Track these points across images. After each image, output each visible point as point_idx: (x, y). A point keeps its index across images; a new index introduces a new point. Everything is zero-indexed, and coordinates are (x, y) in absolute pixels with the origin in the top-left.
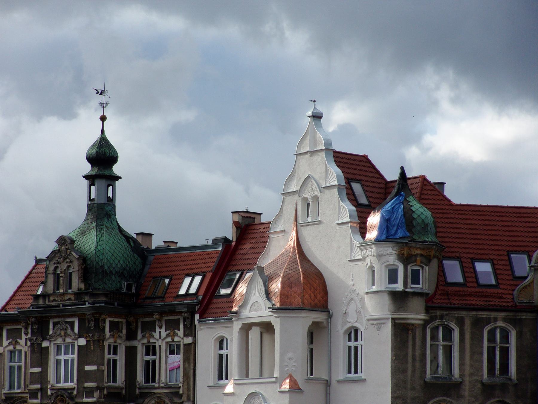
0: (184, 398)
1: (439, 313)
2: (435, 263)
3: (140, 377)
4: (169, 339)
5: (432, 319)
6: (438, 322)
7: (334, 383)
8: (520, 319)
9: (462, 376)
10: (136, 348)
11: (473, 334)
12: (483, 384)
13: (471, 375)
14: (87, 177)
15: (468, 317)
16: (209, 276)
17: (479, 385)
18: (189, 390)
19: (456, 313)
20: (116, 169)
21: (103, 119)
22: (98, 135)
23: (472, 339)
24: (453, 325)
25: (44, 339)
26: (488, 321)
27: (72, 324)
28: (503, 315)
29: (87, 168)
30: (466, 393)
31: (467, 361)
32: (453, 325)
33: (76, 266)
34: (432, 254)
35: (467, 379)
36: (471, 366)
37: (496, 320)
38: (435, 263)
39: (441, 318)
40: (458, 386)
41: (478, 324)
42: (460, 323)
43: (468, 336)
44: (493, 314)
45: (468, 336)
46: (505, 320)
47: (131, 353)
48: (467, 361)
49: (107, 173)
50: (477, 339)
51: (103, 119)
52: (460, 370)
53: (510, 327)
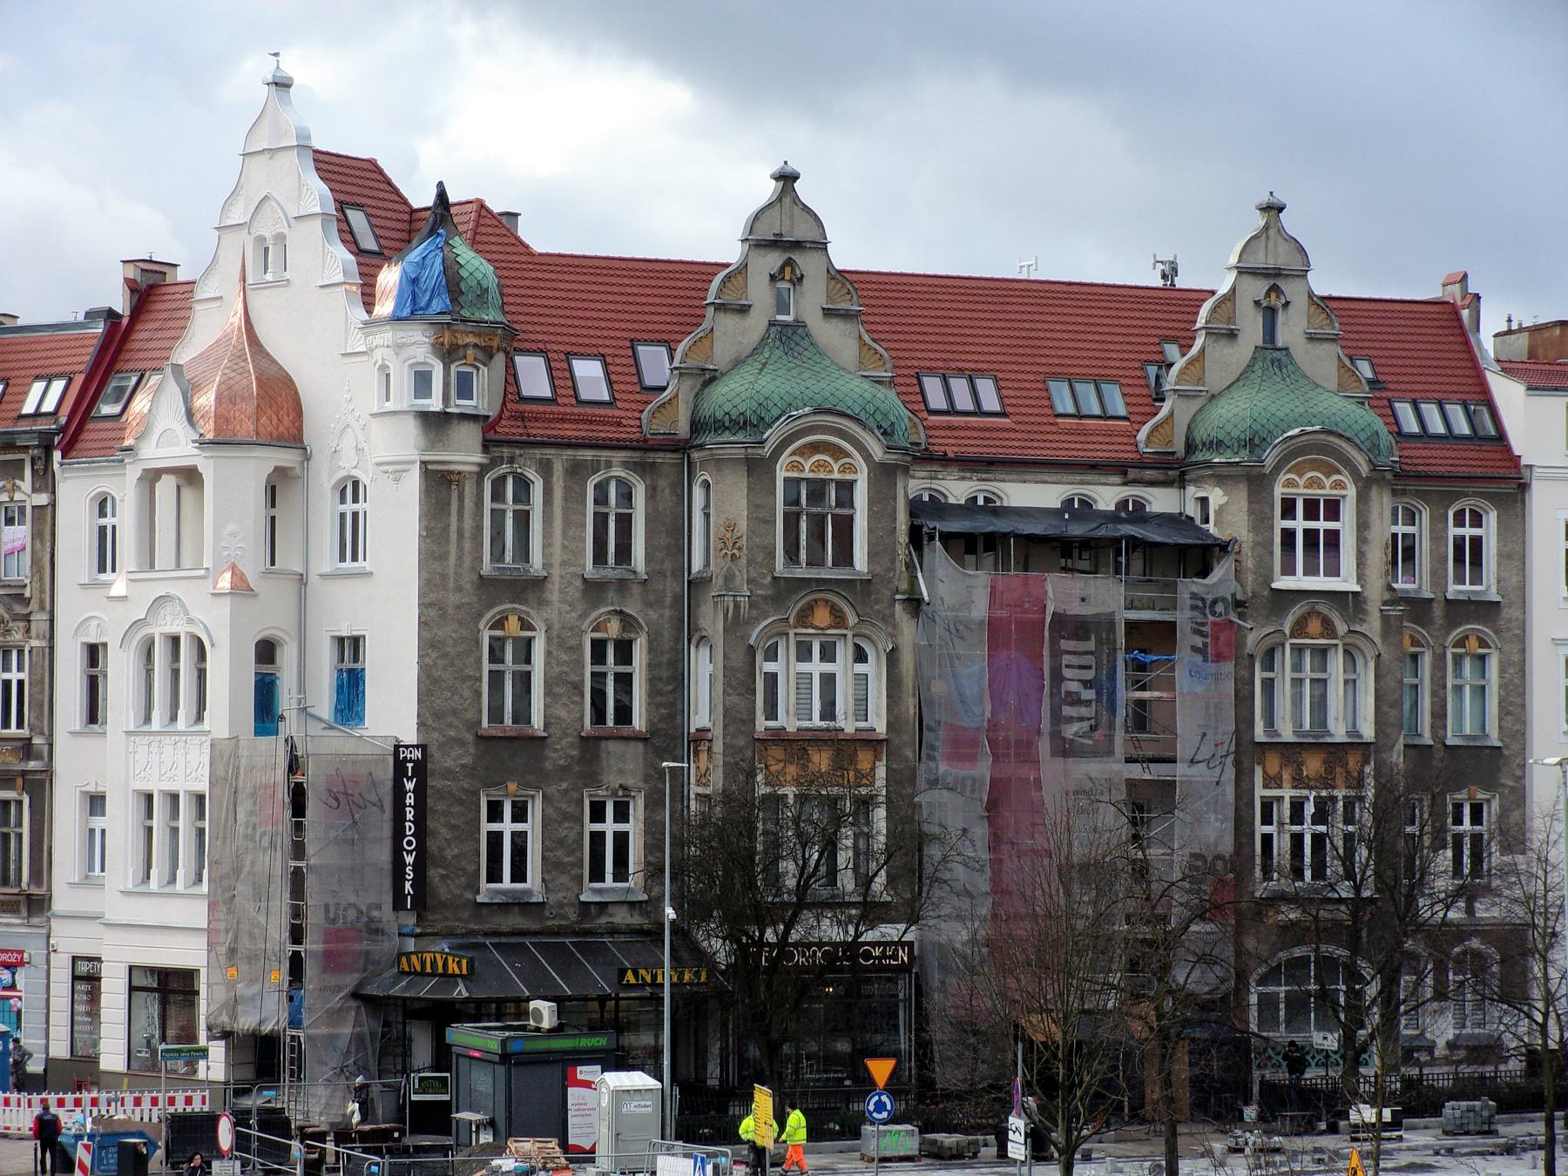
0: (34, 605)
1: (506, 452)
2: (500, 359)
5: (494, 463)
6: (504, 469)
7: (313, 578)
12: (585, 580)
13: (564, 564)
15: (560, 461)
16: (79, 380)
17: (578, 583)
18: (42, 591)
23: (566, 500)
24: (531, 474)
26: (595, 467)
28: (620, 456)
34: (495, 344)
35: (556, 572)
36: (564, 547)
37: (609, 465)
38: (500, 359)
39: (511, 460)
40: (540, 583)
41: (577, 472)
42: (545, 469)
43: (558, 494)
44: (604, 455)
45: (558, 494)
46: (626, 465)
50: (574, 498)
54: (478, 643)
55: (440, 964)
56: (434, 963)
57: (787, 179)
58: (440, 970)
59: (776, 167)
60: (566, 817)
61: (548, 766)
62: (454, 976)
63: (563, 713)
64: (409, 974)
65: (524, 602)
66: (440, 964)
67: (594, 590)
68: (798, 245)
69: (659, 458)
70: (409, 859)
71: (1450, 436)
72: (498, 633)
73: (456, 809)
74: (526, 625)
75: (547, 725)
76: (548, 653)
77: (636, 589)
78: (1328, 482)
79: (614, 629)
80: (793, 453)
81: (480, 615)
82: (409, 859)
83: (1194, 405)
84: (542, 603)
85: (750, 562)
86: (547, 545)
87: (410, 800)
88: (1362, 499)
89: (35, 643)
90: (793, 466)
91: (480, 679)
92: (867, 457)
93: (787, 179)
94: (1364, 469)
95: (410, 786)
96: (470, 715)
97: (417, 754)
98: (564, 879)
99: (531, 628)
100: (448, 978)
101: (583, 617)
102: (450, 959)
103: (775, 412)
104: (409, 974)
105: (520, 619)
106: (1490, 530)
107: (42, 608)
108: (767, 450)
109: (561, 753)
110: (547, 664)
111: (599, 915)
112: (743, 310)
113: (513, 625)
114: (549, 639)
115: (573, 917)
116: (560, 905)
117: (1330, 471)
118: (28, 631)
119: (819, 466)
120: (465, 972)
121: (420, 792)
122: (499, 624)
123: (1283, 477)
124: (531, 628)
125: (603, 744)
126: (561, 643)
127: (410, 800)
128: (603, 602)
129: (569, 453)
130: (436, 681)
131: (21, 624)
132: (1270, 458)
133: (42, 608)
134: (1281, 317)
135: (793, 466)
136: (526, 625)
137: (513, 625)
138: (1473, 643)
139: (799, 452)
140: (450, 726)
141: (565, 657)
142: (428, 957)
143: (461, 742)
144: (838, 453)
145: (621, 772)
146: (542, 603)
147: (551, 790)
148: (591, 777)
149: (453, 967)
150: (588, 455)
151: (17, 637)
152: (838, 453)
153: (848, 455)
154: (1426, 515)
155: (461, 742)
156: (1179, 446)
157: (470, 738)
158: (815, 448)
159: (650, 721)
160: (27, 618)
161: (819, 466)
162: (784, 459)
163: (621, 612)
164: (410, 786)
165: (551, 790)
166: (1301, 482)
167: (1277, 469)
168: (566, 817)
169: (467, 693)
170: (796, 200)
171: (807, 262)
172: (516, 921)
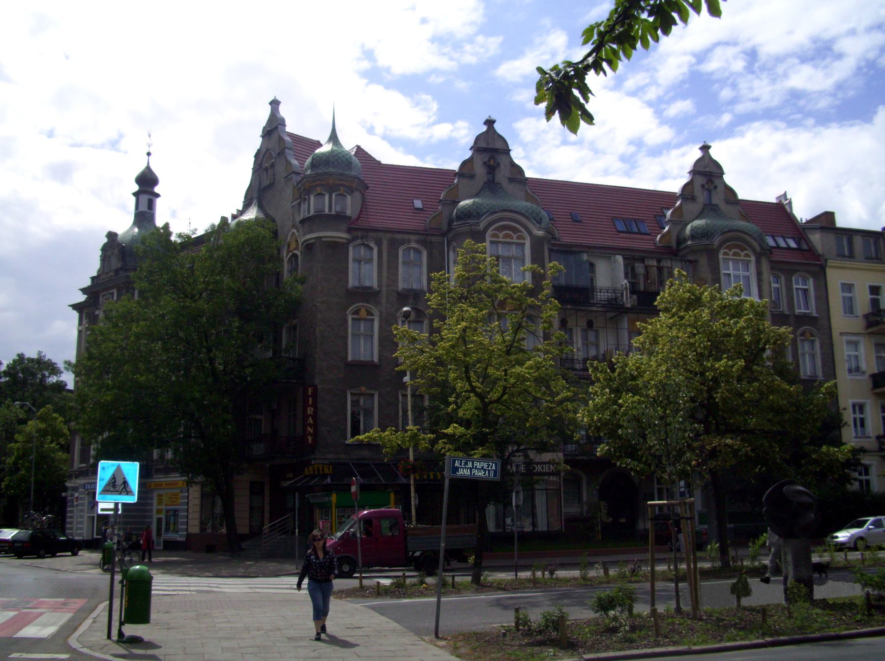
1: (360, 234)
6: (359, 241)
8: (431, 242)
9: (380, 286)
12: (398, 293)
14: (135, 194)
19: (374, 234)
20: (157, 190)
21: (149, 154)
22: (146, 165)
24: (372, 244)
25: (97, 309)
26: (403, 242)
27: (112, 294)
29: (136, 188)
30: (384, 301)
31: (385, 274)
32: (372, 244)
33: (116, 252)
34: (354, 185)
35: (384, 289)
37: (409, 241)
42: (379, 243)
43: (385, 254)
44: (406, 237)
45: (385, 254)
46: (417, 242)
48: (385, 274)
49: (148, 189)
51: (149, 154)
52: (378, 281)
54: (346, 321)
56: (318, 470)
57: (490, 123)
59: (486, 117)
65: (368, 302)
68: (496, 151)
71: (789, 248)
72: (356, 316)
75: (380, 360)
76: (381, 327)
78: (742, 254)
80: (494, 230)
81: (347, 307)
83: (679, 227)
88: (758, 262)
90: (494, 236)
91: (347, 337)
92: (530, 233)
93: (490, 123)
94: (758, 249)
99: (372, 315)
103: (484, 210)
105: (367, 310)
106: (811, 285)
108: (482, 226)
112: (472, 177)
113: (363, 313)
114: (381, 320)
117: (743, 249)
119: (506, 236)
122: (357, 312)
123: (722, 251)
124: (372, 315)
129: (389, 235)
132: (716, 241)
134: (713, 193)
135: (494, 236)
136: (369, 313)
137: (363, 313)
138: (808, 334)
139: (496, 229)
144: (515, 230)
149: (326, 470)
150: (399, 236)
152: (515, 230)
153: (520, 231)
154: (783, 279)
156: (674, 244)
162: (490, 232)
166: (731, 253)
167: (720, 246)
170: (495, 132)
171: (502, 159)
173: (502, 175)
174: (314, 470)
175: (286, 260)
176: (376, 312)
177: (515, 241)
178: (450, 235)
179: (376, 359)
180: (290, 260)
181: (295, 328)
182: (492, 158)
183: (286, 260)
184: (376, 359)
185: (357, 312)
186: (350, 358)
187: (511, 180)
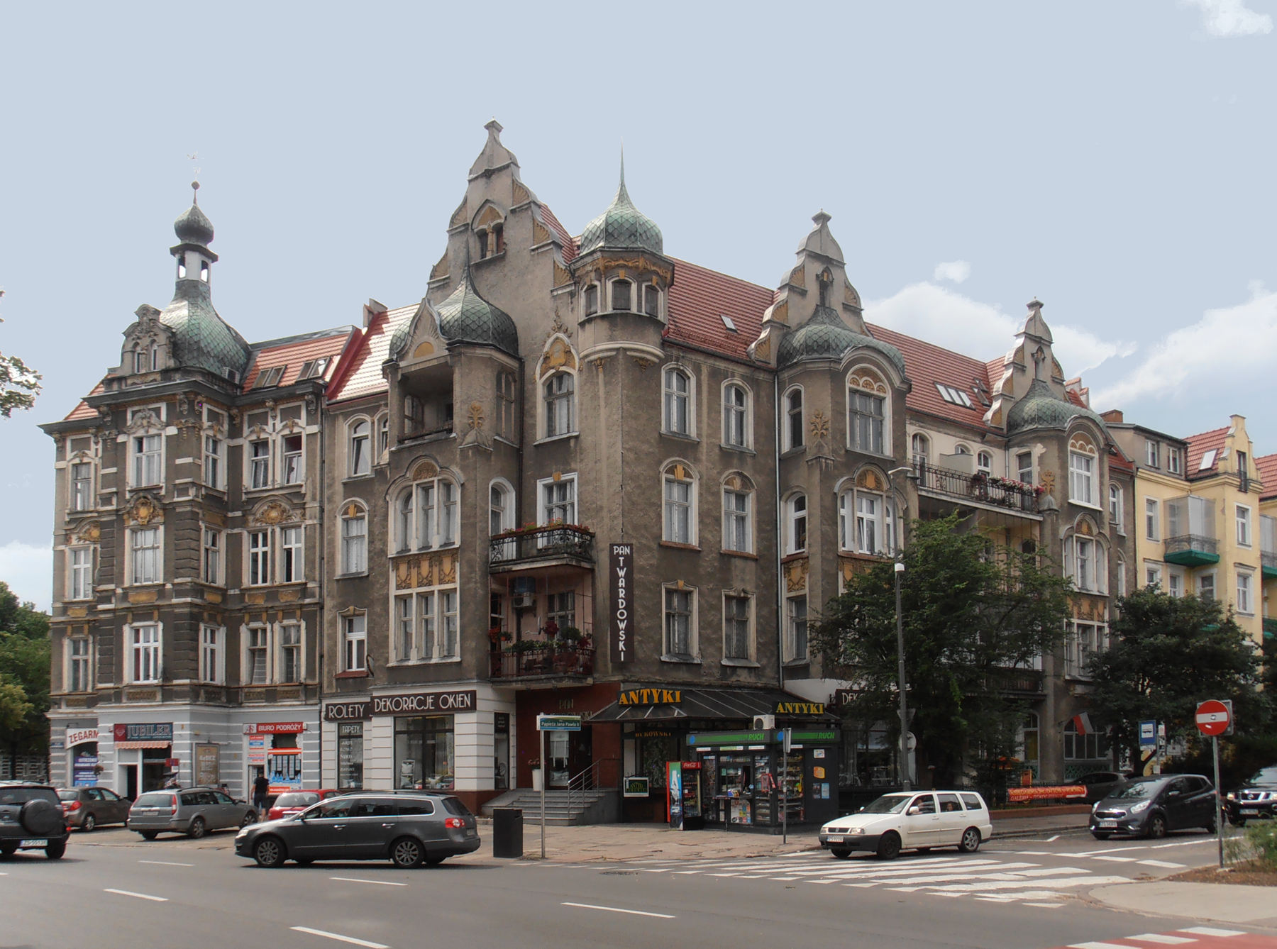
0: (308, 498)
3: (247, 481)
4: (287, 432)
5: (667, 359)
7: (527, 452)
9: (699, 435)
10: (241, 447)
11: (710, 387)
12: (721, 448)
13: (709, 436)
15: (706, 365)
17: (717, 450)
19: (693, 357)
23: (709, 392)
24: (689, 372)
28: (741, 370)
30: (704, 458)
35: (704, 440)
36: (709, 425)
37: (733, 376)
39: (677, 360)
40: (695, 445)
41: (716, 376)
42: (698, 371)
43: (705, 388)
44: (731, 367)
45: (705, 388)
46: (743, 377)
47: (235, 454)
53: (747, 388)
54: (659, 481)
55: (656, 696)
56: (650, 696)
58: (656, 701)
60: (712, 607)
61: (702, 571)
62: (668, 704)
63: (709, 536)
64: (625, 706)
66: (656, 696)
67: (728, 456)
69: (762, 376)
70: (622, 626)
72: (671, 476)
73: (647, 595)
74: (687, 474)
76: (701, 495)
77: (749, 460)
79: (738, 483)
81: (660, 462)
82: (622, 626)
84: (697, 460)
85: (834, 438)
86: (699, 421)
87: (622, 583)
89: (309, 522)
95: (621, 573)
96: (655, 530)
97: (627, 550)
98: (711, 650)
100: (661, 706)
101: (720, 473)
102: (665, 692)
104: (625, 706)
107: (314, 499)
108: (841, 367)
109: (709, 563)
110: (700, 502)
111: (732, 675)
114: (701, 485)
115: (717, 675)
116: (710, 667)
118: (304, 515)
120: (678, 700)
121: (628, 577)
122: (671, 470)
124: (691, 477)
125: (733, 560)
126: (709, 492)
127: (622, 583)
128: (727, 466)
129: (711, 361)
130: (633, 504)
131: (299, 512)
133: (314, 499)
136: (687, 474)
140: (643, 536)
141: (710, 499)
142: (645, 692)
143: (649, 549)
144: (876, 378)
145: (743, 580)
146: (697, 460)
147: (704, 588)
148: (726, 583)
149: (667, 698)
150: (722, 365)
151: (296, 520)
152: (876, 378)
155: (649, 549)
157: (655, 546)
158: (865, 372)
159: (758, 548)
160: (303, 507)
161: (867, 384)
163: (740, 474)
164: (621, 573)
165: (704, 588)
168: (712, 607)
169: (652, 514)
171: (836, 273)
172: (684, 676)
173: (836, 299)
174: (641, 698)
175: (540, 382)
176: (694, 472)
177: (875, 392)
178: (786, 375)
179: (694, 541)
180: (549, 386)
181: (562, 486)
182: (827, 270)
183: (540, 382)
184: (694, 541)
185: (671, 470)
186: (664, 539)
187: (846, 307)
